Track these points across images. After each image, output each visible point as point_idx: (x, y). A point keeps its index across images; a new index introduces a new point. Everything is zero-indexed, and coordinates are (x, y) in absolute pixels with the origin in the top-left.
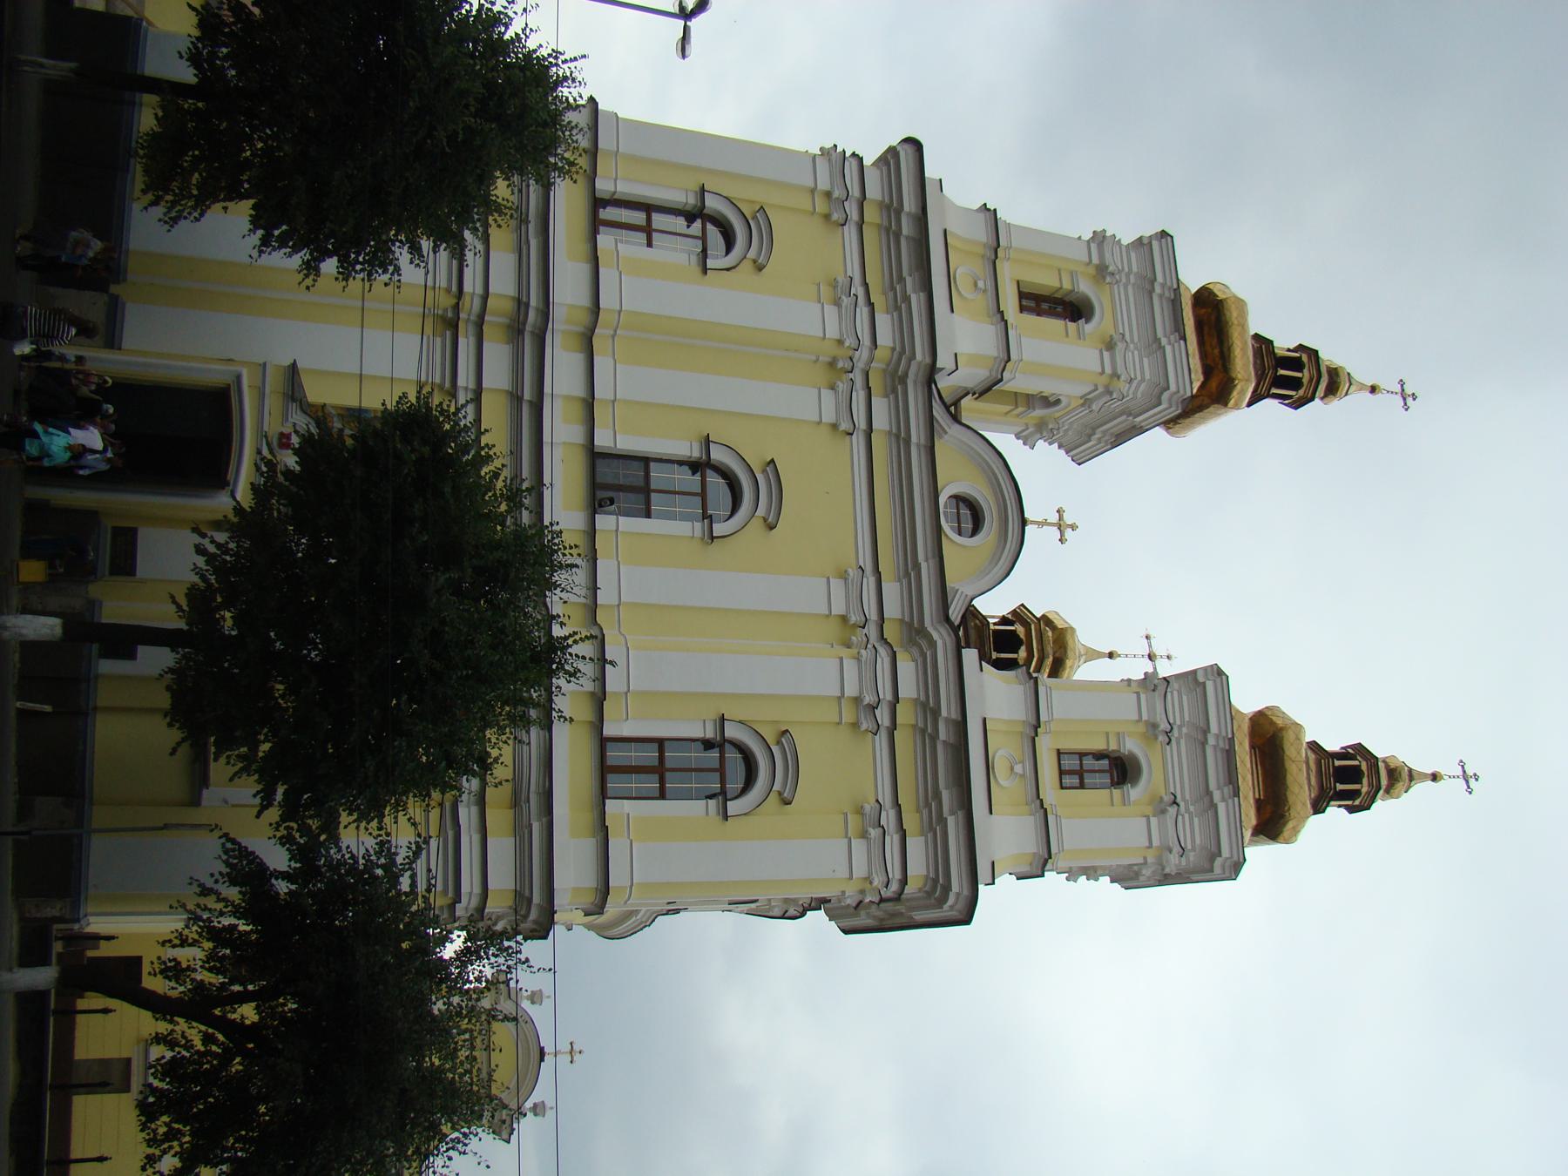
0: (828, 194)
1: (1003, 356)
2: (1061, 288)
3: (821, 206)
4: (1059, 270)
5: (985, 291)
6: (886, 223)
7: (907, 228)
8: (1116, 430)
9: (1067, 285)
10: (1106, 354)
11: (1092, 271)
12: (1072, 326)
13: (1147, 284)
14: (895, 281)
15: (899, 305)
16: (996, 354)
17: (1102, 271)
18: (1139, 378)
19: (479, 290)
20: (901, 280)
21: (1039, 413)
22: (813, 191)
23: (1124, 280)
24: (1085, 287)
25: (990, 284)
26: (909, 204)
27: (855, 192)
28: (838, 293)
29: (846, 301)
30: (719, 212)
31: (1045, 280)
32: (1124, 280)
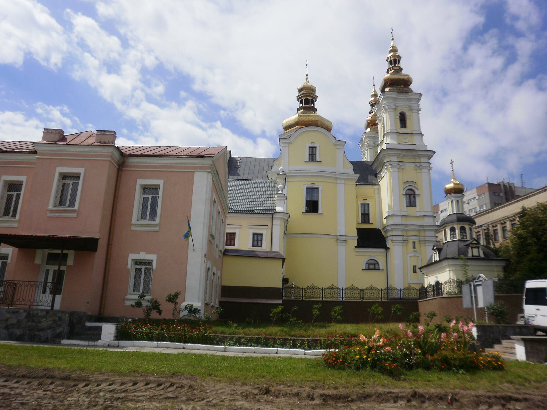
0: (398, 168)
10: (414, 111)
12: (407, 118)
14: (414, 157)
15: (419, 156)
17: (395, 109)
20: (413, 155)
24: (399, 113)
25: (404, 135)
26: (399, 152)
27: (397, 163)
29: (421, 168)
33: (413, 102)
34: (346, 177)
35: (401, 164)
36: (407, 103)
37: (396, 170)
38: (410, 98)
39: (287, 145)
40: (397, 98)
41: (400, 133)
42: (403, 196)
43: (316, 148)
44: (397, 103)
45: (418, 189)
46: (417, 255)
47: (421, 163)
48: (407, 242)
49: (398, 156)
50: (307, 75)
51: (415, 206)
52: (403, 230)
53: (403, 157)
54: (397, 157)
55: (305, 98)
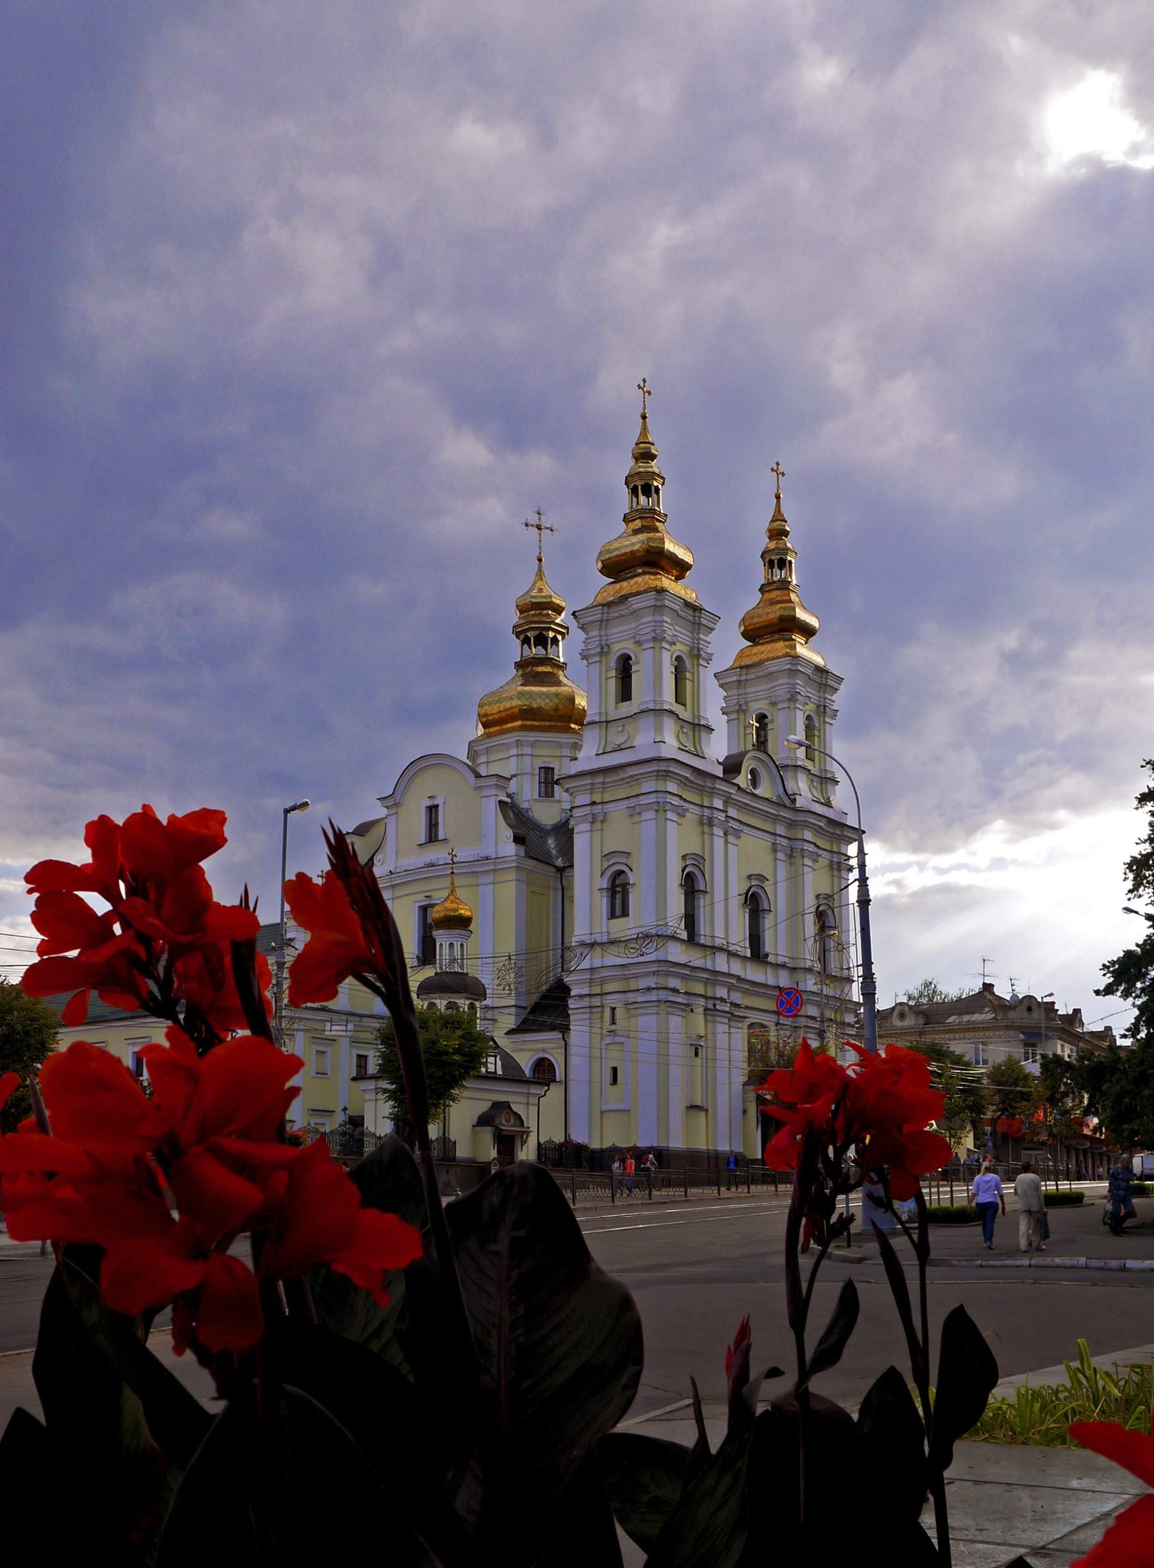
0: (592, 823)
1: (652, 713)
2: (616, 677)
3: (598, 825)
4: (607, 679)
5: (623, 725)
6: (601, 790)
7: (599, 779)
8: (690, 612)
9: (613, 673)
11: (604, 659)
13: (604, 623)
16: (652, 717)
18: (653, 624)
19: (655, 992)
20: (623, 779)
21: (688, 664)
22: (591, 831)
23: (604, 638)
24: (612, 661)
26: (588, 781)
28: (633, 812)
30: (608, 880)
31: (612, 686)
32: (604, 638)
33: (644, 620)
34: (493, 867)
35: (597, 809)
36: (633, 626)
37: (587, 826)
38: (635, 611)
39: (394, 810)
40: (607, 620)
41: (607, 722)
42: (599, 893)
43: (437, 806)
44: (609, 631)
45: (631, 870)
46: (618, 1039)
47: (641, 798)
48: (599, 1009)
49: (591, 789)
50: (540, 560)
51: (628, 915)
52: (591, 982)
53: (604, 788)
54: (591, 793)
55: (522, 637)
